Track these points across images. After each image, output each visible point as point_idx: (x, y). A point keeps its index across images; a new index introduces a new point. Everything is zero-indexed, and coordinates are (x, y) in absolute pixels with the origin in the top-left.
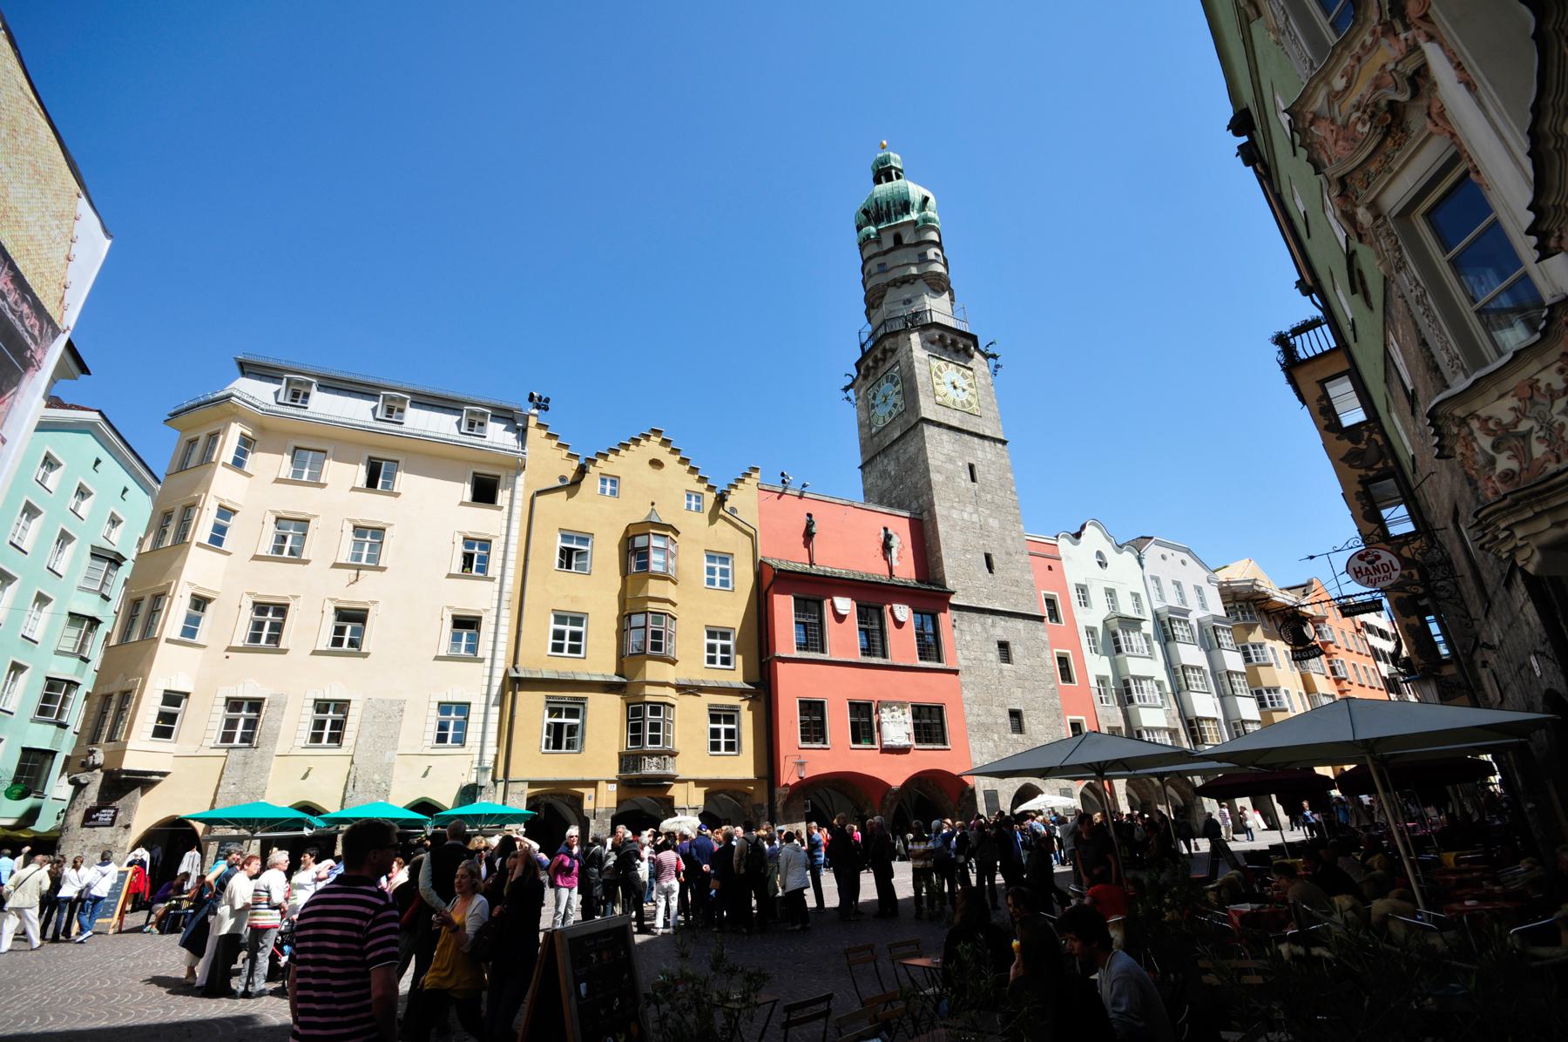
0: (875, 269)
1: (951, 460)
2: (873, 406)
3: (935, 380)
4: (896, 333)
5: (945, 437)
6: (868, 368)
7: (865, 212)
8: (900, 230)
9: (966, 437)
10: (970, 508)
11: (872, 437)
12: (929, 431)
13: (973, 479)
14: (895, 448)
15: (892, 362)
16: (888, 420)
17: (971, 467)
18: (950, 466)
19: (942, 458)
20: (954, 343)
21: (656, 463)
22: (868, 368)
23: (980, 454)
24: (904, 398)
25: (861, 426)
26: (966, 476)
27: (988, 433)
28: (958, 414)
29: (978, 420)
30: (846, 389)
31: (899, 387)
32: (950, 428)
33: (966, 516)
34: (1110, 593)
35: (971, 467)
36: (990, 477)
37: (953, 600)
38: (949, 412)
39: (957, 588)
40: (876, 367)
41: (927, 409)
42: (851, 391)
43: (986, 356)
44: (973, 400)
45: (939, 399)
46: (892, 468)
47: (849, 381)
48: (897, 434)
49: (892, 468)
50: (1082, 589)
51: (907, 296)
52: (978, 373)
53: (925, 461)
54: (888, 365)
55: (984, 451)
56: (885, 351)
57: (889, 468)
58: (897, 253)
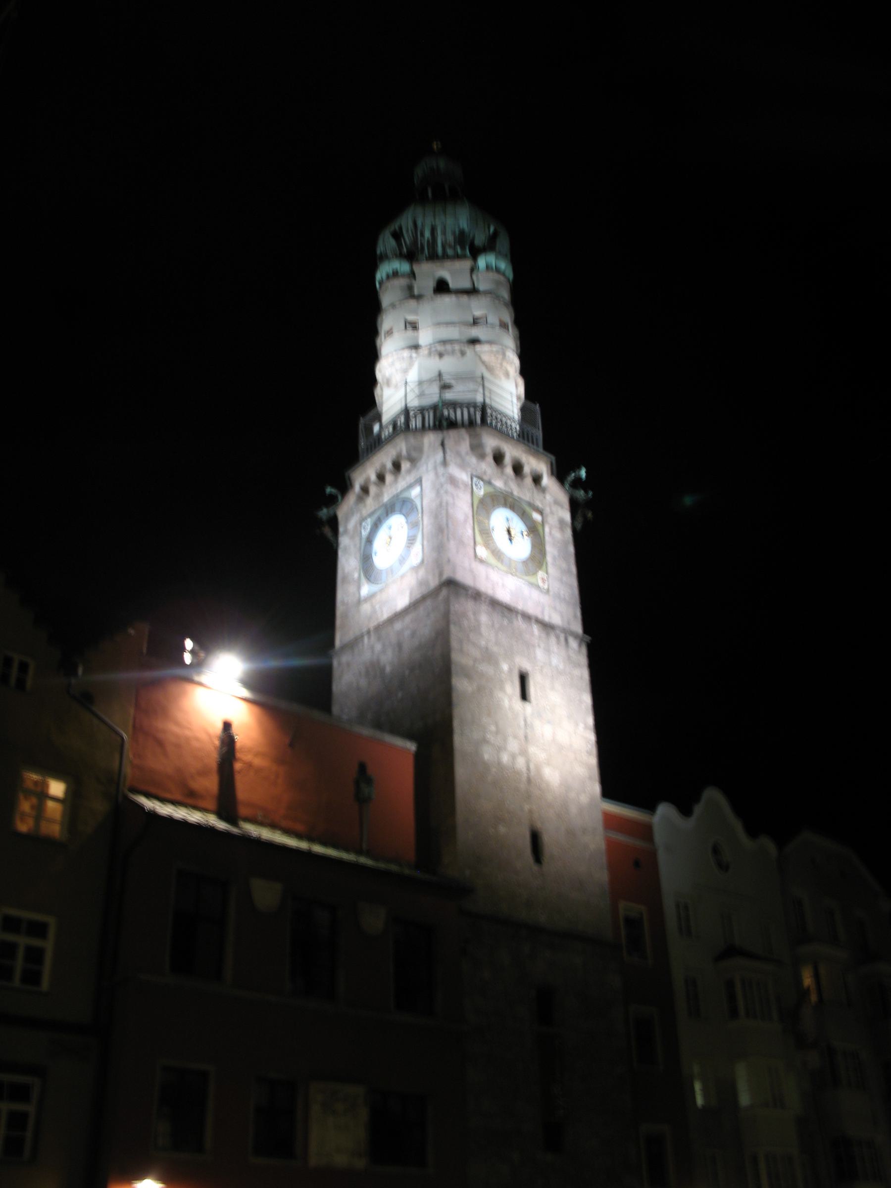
9: (520, 623)
13: (524, 696)
15: (410, 479)
23: (540, 654)
26: (514, 689)
52: (552, 520)
54: (402, 483)
55: (548, 651)
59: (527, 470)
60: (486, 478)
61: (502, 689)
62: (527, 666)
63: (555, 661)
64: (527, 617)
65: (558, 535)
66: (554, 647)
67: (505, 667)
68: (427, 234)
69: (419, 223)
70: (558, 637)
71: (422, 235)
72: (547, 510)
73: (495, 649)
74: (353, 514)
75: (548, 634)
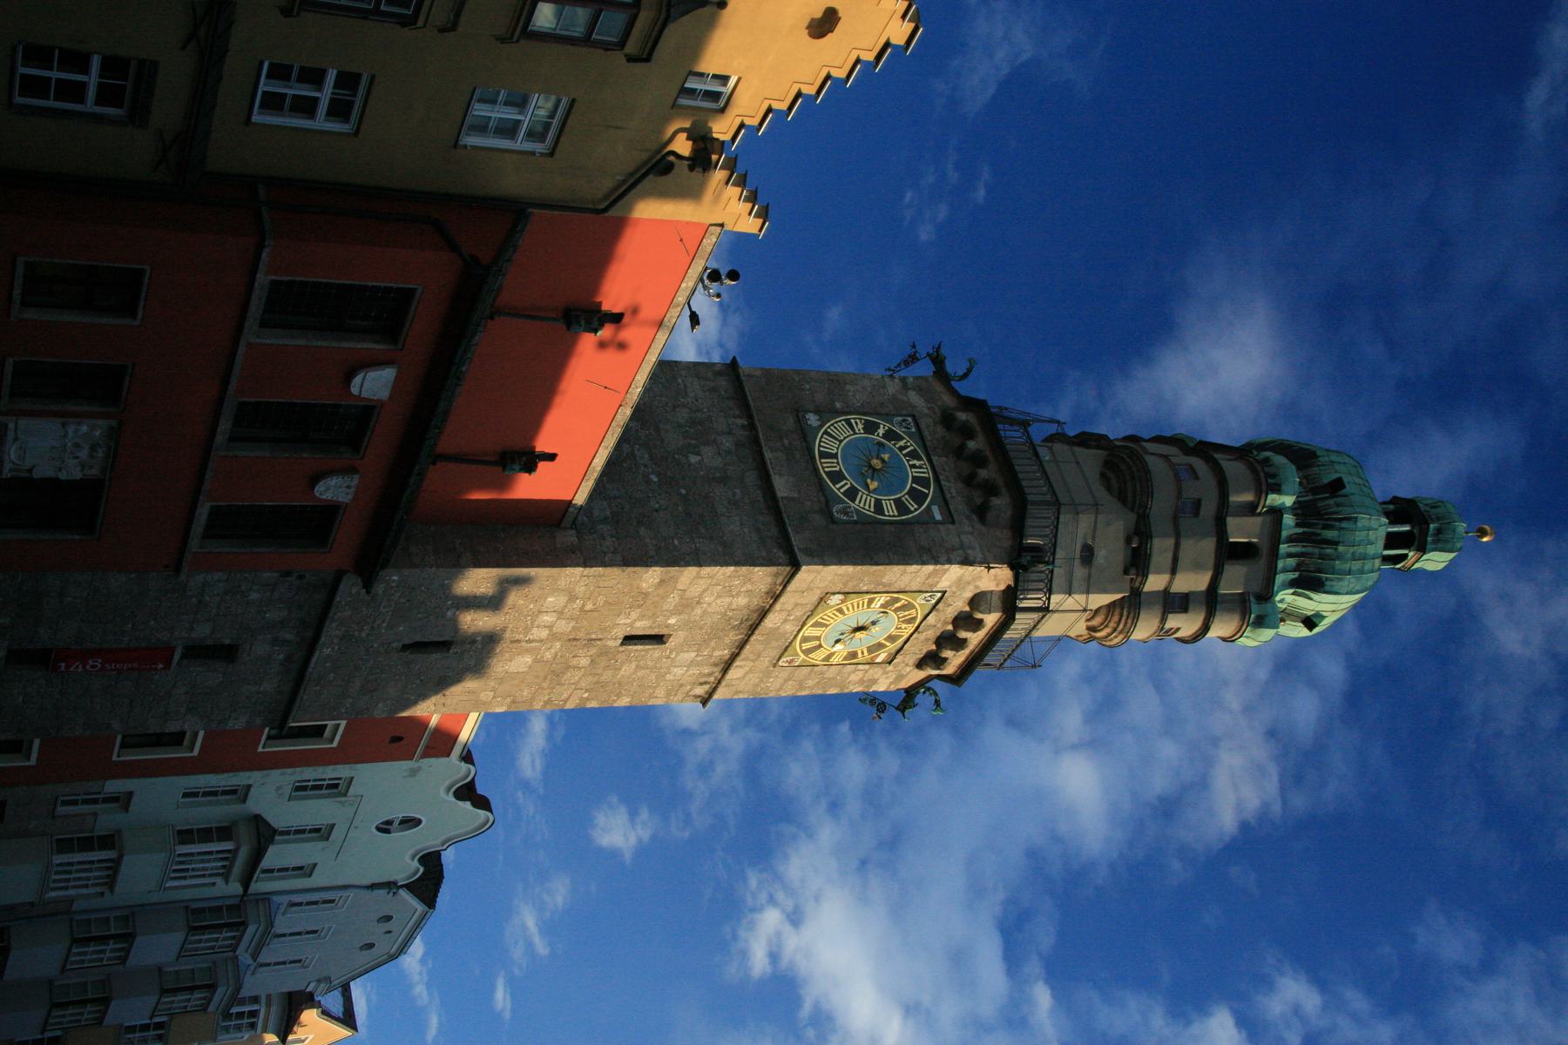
0: (1191, 491)
1: (686, 605)
2: (870, 428)
3: (883, 599)
4: (1018, 527)
5: (742, 601)
6: (967, 432)
7: (1337, 485)
8: (1262, 563)
9: (734, 637)
10: (563, 626)
11: (799, 413)
12: (761, 577)
13: (630, 639)
14: (751, 478)
15: (958, 505)
16: (825, 467)
17: (659, 639)
18: (673, 600)
19: (695, 591)
20: (960, 644)
21: (825, 24)
22: (967, 432)
24: (864, 521)
25: (836, 382)
26: (642, 627)
27: (733, 674)
28: (790, 628)
29: (765, 661)
30: (937, 360)
31: (890, 510)
32: (763, 614)
33: (547, 618)
34: (321, 833)
35: (659, 639)
36: (627, 670)
37: (351, 586)
38: (799, 613)
39: (379, 589)
40: (959, 452)
41: (814, 577)
42: (925, 369)
43: (910, 693)
44: (818, 657)
45: (835, 600)
46: (707, 458)
47: (954, 366)
48: (782, 486)
49: (707, 458)
50: (335, 788)
51: (1101, 556)
52: (876, 672)
53: (698, 560)
54: (953, 488)
55: (692, 664)
56: (990, 490)
57: (708, 451)
58: (1208, 546)
59: (947, 653)
60: (940, 606)
61: (642, 617)
62: (671, 643)
63: (678, 671)
64: (742, 645)
65: (853, 677)
66: (695, 671)
67: (672, 621)
68: (1330, 534)
69: (1344, 525)
70: (710, 675)
71: (1326, 527)
72: (890, 668)
73: (698, 611)
74: (927, 401)
75: (716, 665)
